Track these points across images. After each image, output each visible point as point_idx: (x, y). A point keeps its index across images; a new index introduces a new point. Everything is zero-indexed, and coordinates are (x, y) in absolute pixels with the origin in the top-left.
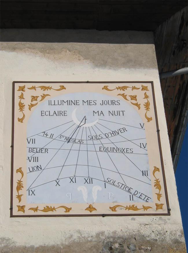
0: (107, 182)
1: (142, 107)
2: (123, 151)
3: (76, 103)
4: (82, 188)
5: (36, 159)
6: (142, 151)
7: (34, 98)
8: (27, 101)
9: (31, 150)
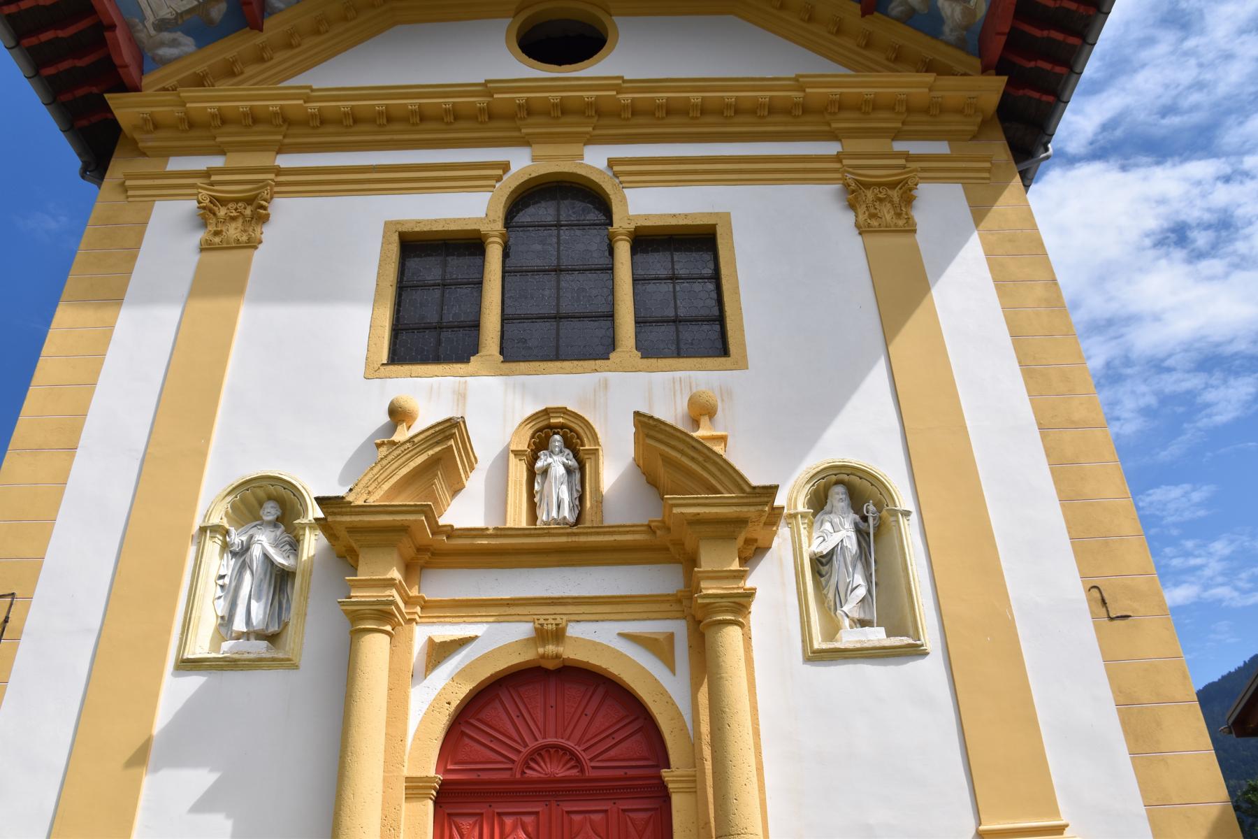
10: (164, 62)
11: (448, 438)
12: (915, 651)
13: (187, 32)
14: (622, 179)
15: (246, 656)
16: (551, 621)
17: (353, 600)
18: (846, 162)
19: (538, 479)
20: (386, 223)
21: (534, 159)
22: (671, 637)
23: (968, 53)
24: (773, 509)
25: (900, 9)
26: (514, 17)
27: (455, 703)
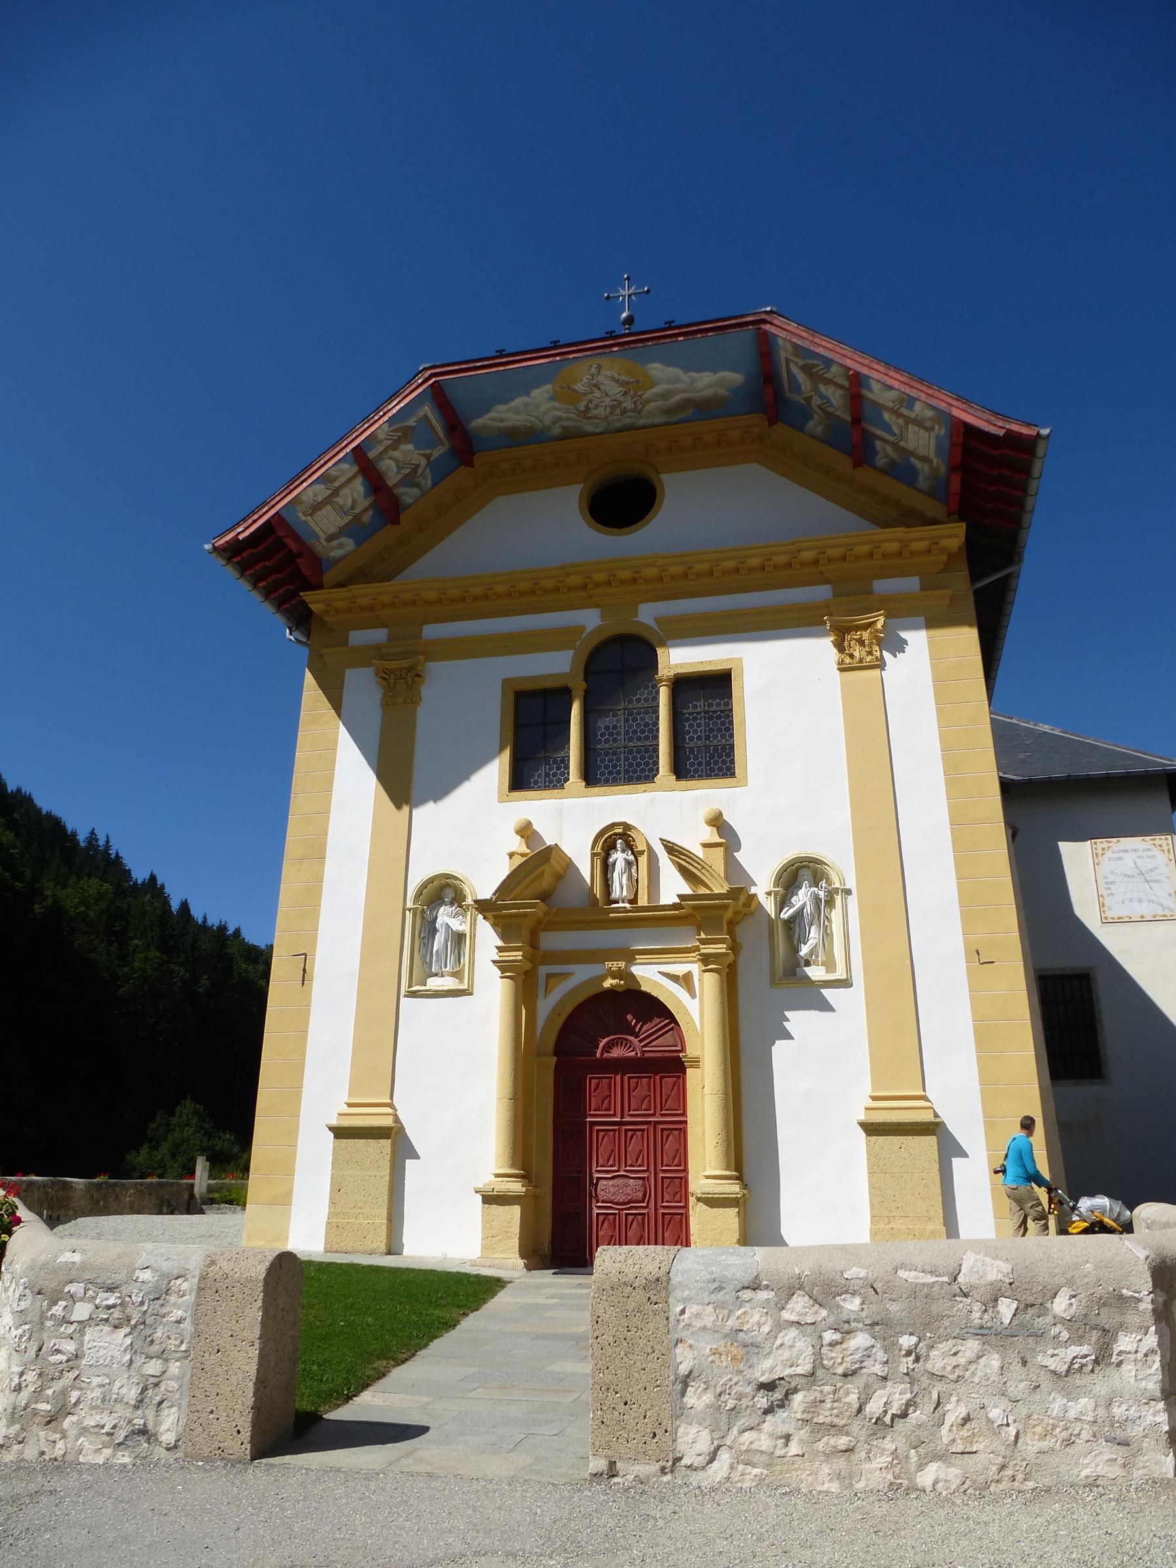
0: (1151, 901)
1: (1166, 852)
2: (1156, 881)
3: (1127, 851)
5: (1110, 889)
7: (1103, 849)
8: (1099, 852)
9: (1106, 883)
10: (337, 561)
13: (348, 536)
16: (615, 965)
20: (504, 680)
21: (603, 617)
24: (749, 895)
25: (885, 460)
26: (584, 483)
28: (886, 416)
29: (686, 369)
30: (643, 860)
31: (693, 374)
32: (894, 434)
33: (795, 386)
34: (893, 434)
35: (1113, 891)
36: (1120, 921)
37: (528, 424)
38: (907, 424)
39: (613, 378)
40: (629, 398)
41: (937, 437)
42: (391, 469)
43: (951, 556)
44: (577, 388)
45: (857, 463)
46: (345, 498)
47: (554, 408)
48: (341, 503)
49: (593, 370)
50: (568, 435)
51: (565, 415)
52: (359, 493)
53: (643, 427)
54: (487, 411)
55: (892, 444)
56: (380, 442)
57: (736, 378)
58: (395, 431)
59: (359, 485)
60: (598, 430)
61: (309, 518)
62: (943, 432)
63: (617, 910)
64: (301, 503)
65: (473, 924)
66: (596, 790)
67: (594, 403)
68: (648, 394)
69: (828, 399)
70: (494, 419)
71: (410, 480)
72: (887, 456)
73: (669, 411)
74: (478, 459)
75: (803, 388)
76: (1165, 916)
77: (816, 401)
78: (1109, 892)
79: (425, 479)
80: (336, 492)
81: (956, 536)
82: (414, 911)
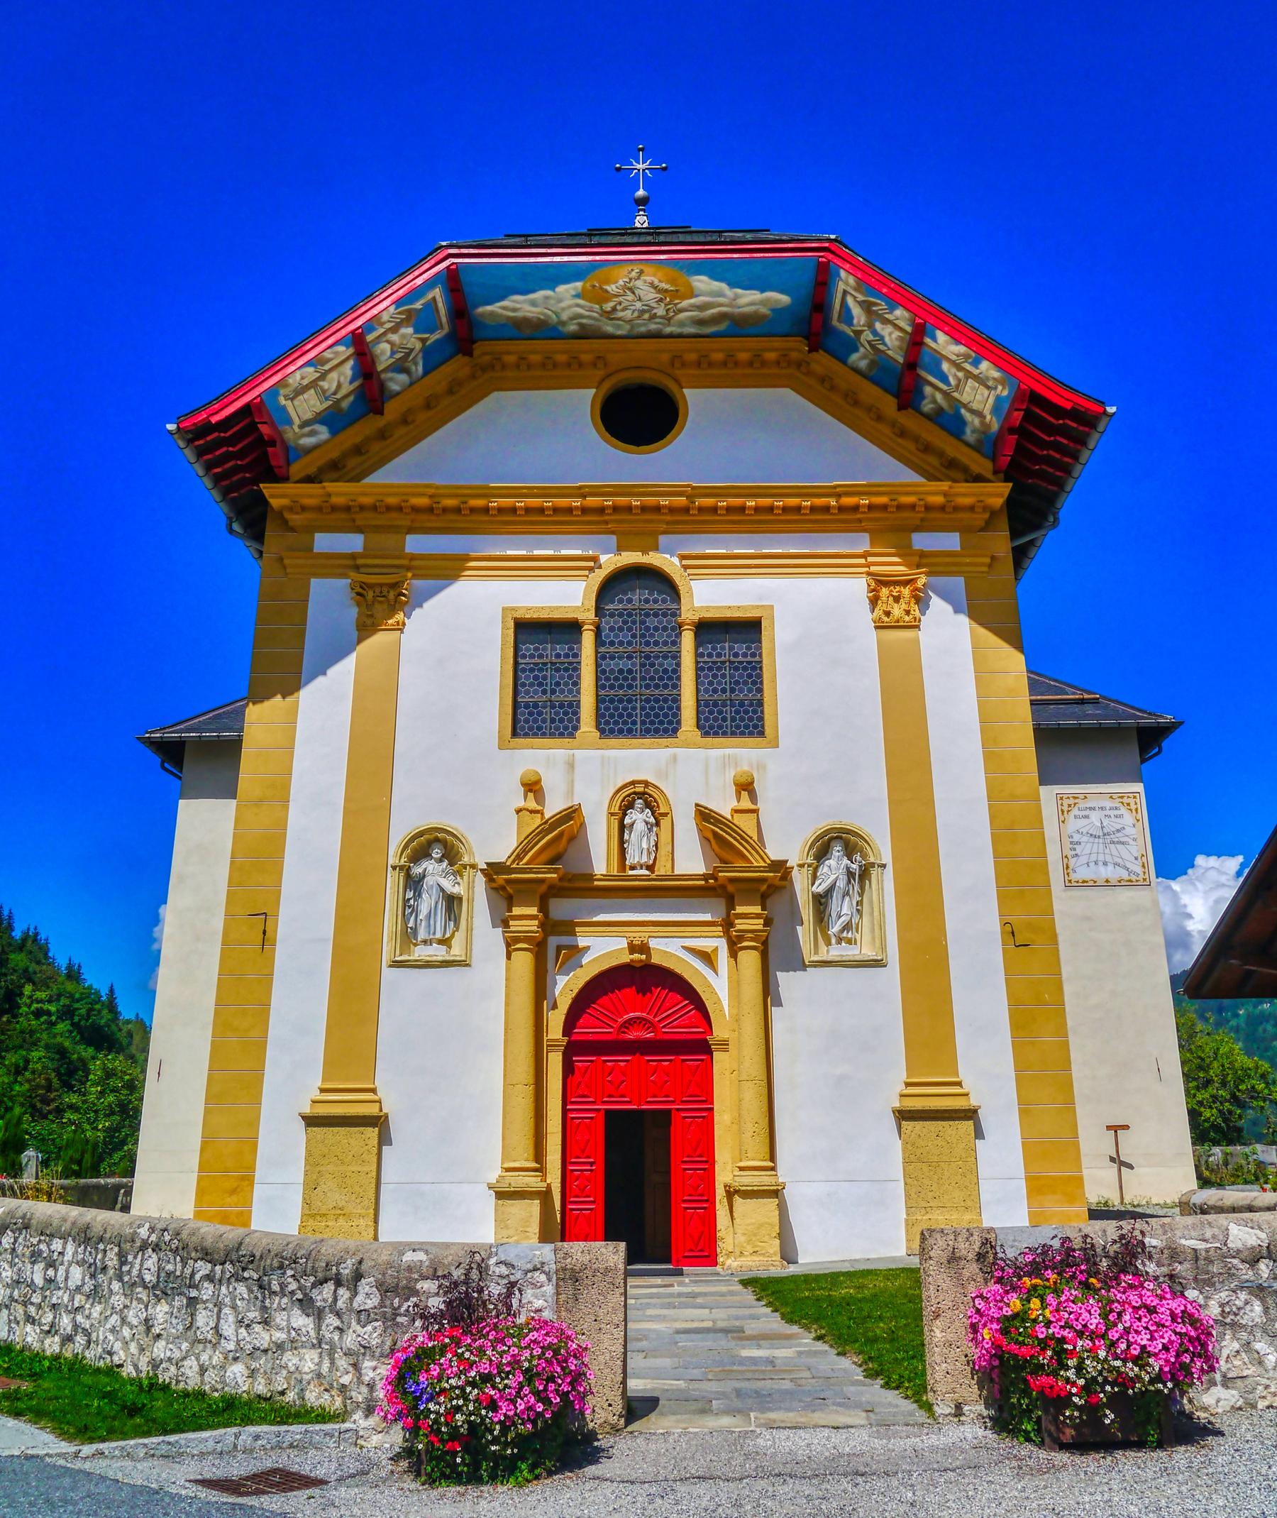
0: (1116, 864)
2: (1123, 843)
3: (1094, 809)
4: (1102, 868)
5: (1075, 849)
6: (1134, 843)
7: (1070, 806)
8: (1065, 808)
9: (1071, 843)
10: (309, 451)
11: (571, 819)
12: (877, 963)
13: (323, 422)
14: (689, 571)
15: (435, 958)
17: (512, 929)
18: (870, 559)
19: (627, 832)
22: (716, 949)
23: (983, 455)
25: (931, 406)
26: (597, 388)
27: (576, 991)
28: (945, 366)
29: (732, 285)
30: (665, 822)
31: (739, 291)
32: (949, 384)
33: (846, 316)
34: (948, 383)
35: (1078, 851)
36: (1084, 884)
37: (542, 317)
38: (967, 378)
39: (652, 285)
40: (663, 305)
41: (998, 398)
42: (383, 353)
43: (994, 513)
44: (608, 288)
45: (901, 407)
46: (329, 384)
47: (578, 305)
48: (326, 387)
49: (634, 274)
50: (586, 334)
51: (587, 313)
52: (346, 377)
53: (671, 336)
54: (502, 298)
55: (945, 394)
56: (382, 324)
57: (784, 299)
58: (399, 313)
59: (348, 369)
60: (619, 333)
61: (289, 402)
62: (1005, 393)
63: (636, 878)
64: (287, 386)
65: (471, 887)
66: (613, 741)
67: (623, 305)
68: (685, 303)
69: (882, 338)
70: (504, 308)
71: (400, 367)
72: (934, 401)
73: (701, 322)
74: (478, 349)
75: (855, 321)
76: (1131, 881)
77: (867, 336)
78: (1074, 853)
79: (416, 364)
80: (323, 376)
81: (1001, 495)
82: (401, 868)
